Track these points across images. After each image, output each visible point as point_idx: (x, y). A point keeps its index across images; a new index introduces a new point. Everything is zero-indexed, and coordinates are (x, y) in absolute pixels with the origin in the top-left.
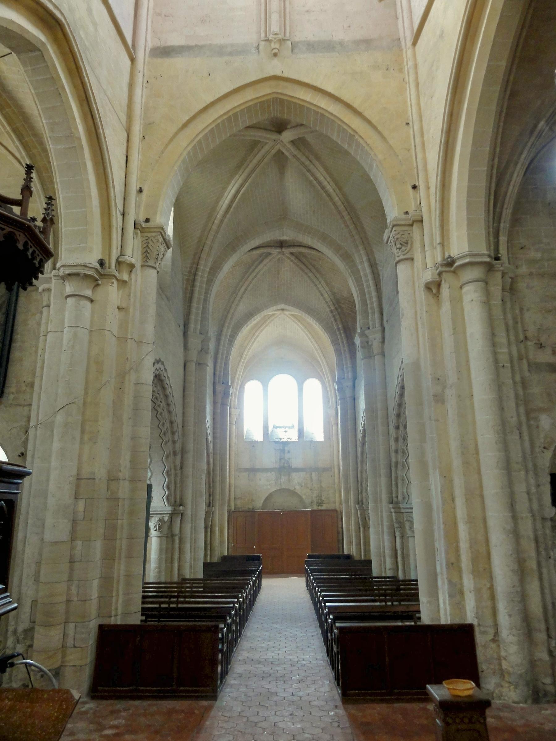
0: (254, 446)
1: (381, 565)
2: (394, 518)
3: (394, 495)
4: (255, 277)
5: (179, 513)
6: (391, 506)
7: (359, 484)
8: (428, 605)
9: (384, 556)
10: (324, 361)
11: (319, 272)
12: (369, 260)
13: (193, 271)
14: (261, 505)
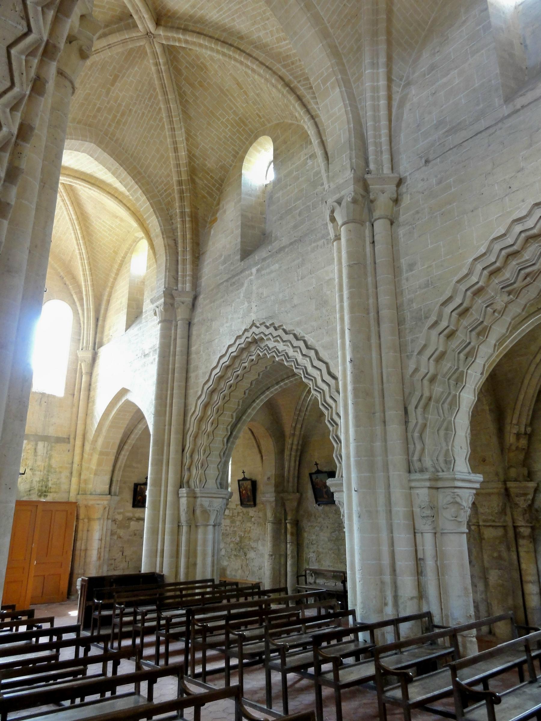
11: (185, 112)
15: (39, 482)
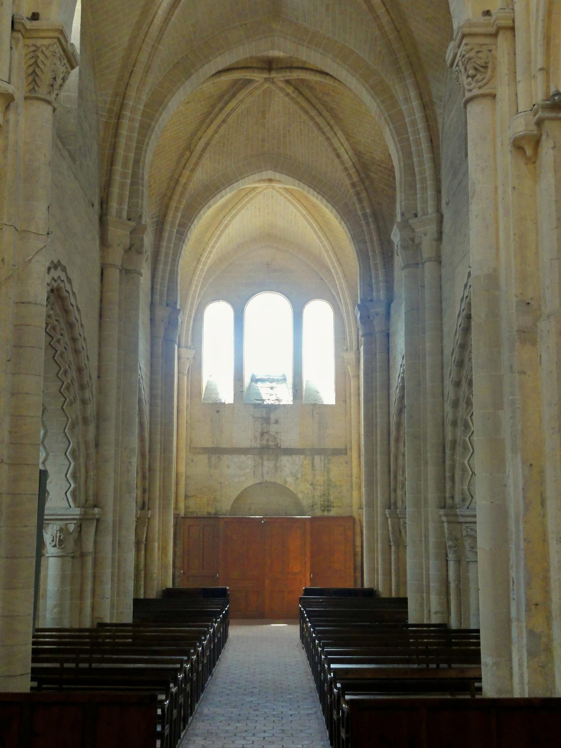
0: (218, 412)
1: (422, 606)
2: (446, 531)
3: (447, 495)
4: (224, 121)
5: (92, 519)
6: (442, 512)
7: (392, 476)
8: (494, 668)
9: (428, 593)
10: (339, 270)
11: (335, 117)
12: (421, 96)
13: (116, 109)
14: (229, 508)
15: (321, 496)
